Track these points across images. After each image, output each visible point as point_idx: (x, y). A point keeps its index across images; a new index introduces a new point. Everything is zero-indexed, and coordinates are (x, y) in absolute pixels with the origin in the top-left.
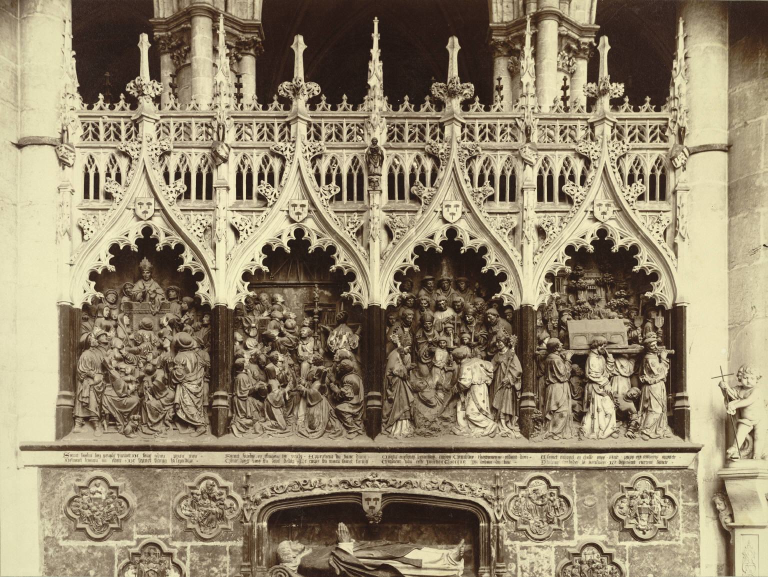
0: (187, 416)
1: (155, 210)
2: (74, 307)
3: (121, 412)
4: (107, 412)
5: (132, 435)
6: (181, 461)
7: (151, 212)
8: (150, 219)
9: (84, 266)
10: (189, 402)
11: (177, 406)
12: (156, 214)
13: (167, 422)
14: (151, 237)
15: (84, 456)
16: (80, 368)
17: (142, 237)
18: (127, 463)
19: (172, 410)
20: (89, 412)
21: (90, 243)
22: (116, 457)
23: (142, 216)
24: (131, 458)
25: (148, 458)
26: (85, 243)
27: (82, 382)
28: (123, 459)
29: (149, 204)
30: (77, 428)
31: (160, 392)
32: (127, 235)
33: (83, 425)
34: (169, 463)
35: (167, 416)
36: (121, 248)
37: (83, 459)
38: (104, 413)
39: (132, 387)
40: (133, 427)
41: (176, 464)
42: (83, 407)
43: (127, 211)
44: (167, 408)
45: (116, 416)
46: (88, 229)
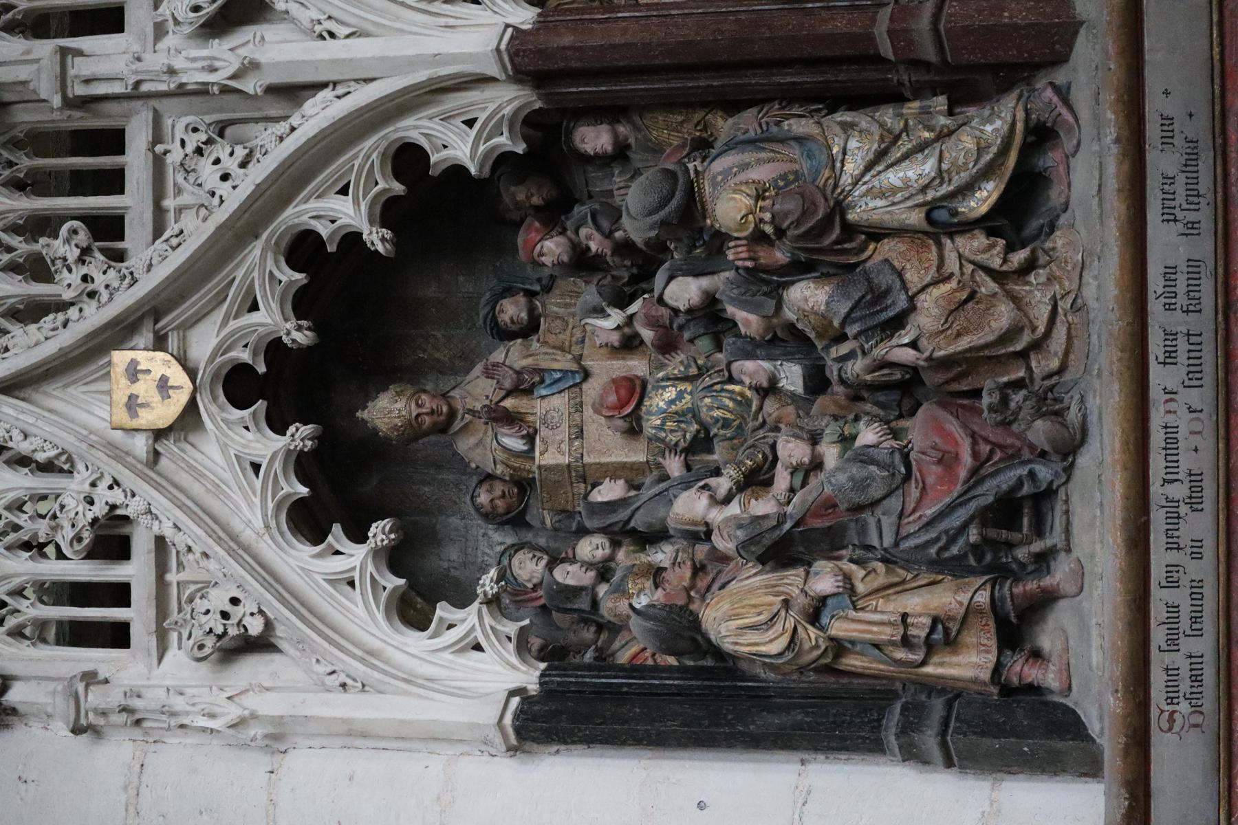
0: (987, 173)
1: (160, 343)
2: (533, 688)
3: (974, 472)
4: (973, 535)
5: (1073, 415)
6: (1193, 193)
7: (159, 364)
8: (192, 373)
9: (375, 644)
10: (921, 169)
11: (942, 215)
12: (173, 342)
13: (1019, 257)
14: (262, 369)
15: (1173, 644)
16: (775, 648)
17: (261, 405)
18: (1207, 443)
19: (960, 241)
20: (971, 611)
21: (276, 610)
22: (1179, 491)
23: (180, 399)
24: (1184, 423)
25: (1182, 346)
26: (280, 631)
27: (839, 647)
28: (1186, 462)
29: (133, 373)
30: (1050, 678)
31: (879, 296)
32: (256, 467)
33: (1037, 655)
34: (1205, 247)
35: (996, 263)
36: (304, 491)
37: (1188, 645)
38: (975, 548)
39: (868, 435)
40: (1039, 414)
41: (1204, 216)
42: (951, 643)
43: (164, 462)
44: (952, 264)
45: (987, 493)
46: (225, 615)
